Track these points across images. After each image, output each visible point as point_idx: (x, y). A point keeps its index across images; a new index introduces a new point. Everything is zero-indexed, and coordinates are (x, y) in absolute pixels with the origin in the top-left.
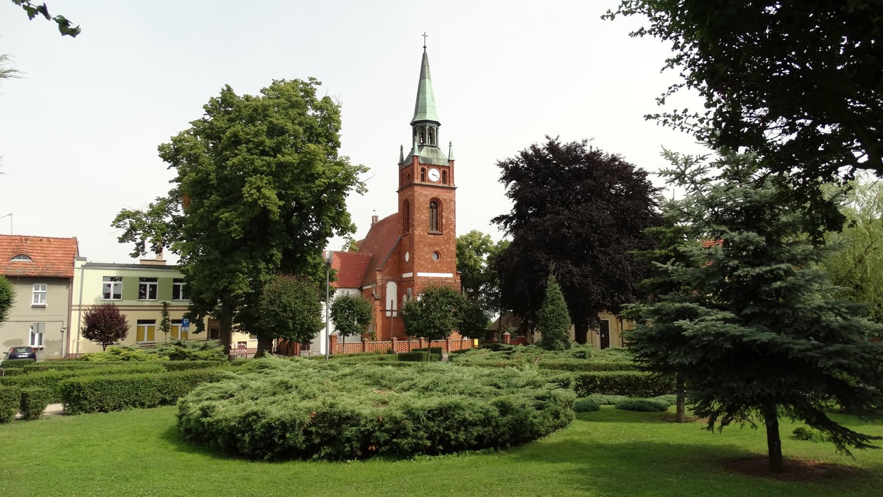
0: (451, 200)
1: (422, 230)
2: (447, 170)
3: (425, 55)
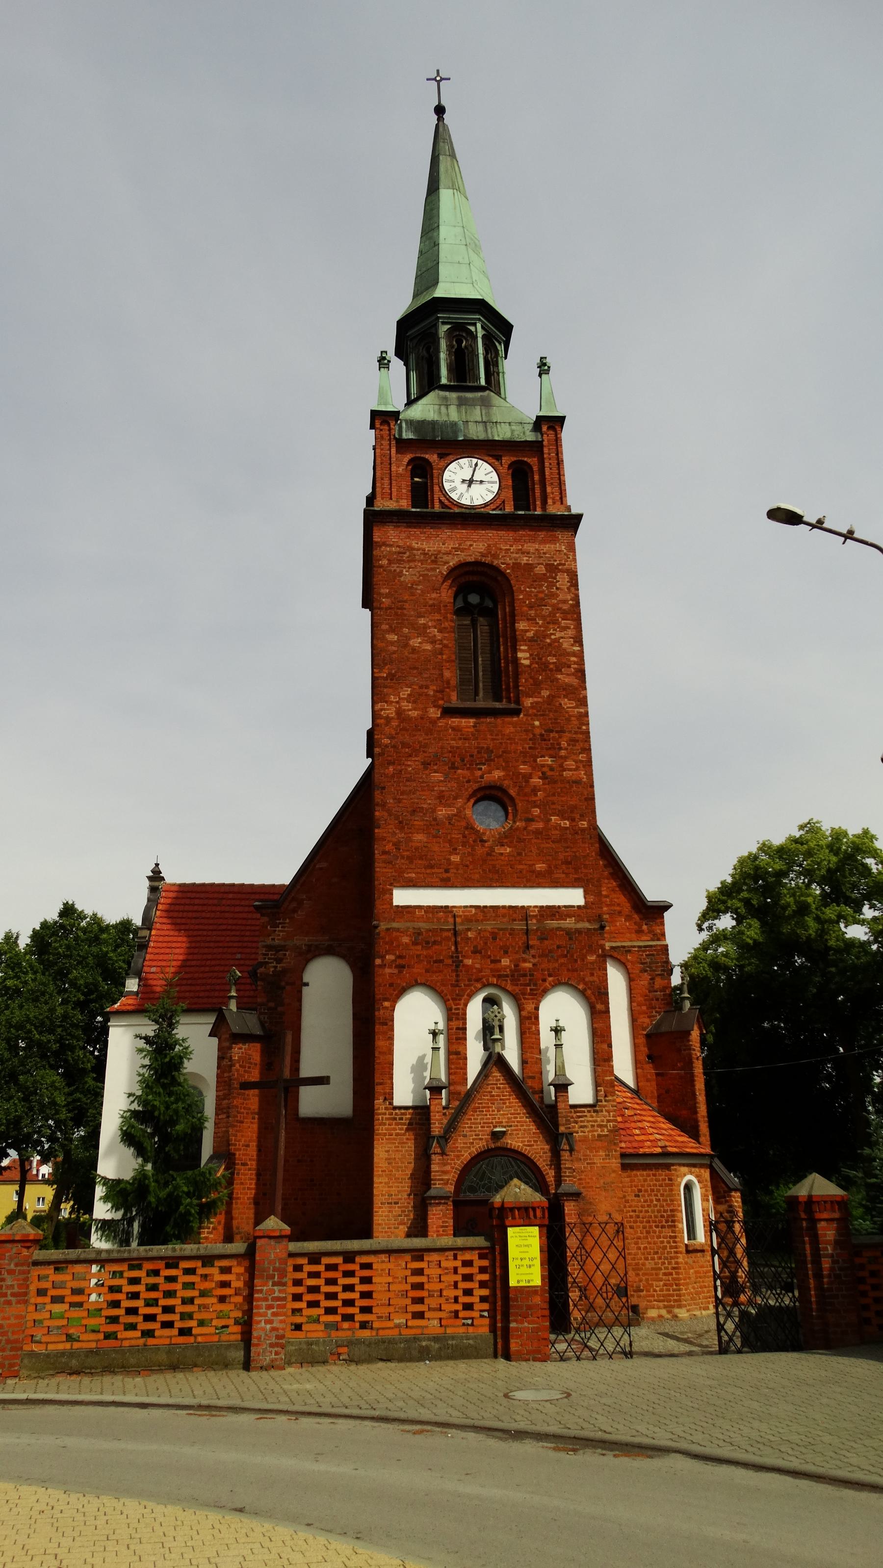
0: (553, 569)
1: (413, 698)
2: (533, 461)
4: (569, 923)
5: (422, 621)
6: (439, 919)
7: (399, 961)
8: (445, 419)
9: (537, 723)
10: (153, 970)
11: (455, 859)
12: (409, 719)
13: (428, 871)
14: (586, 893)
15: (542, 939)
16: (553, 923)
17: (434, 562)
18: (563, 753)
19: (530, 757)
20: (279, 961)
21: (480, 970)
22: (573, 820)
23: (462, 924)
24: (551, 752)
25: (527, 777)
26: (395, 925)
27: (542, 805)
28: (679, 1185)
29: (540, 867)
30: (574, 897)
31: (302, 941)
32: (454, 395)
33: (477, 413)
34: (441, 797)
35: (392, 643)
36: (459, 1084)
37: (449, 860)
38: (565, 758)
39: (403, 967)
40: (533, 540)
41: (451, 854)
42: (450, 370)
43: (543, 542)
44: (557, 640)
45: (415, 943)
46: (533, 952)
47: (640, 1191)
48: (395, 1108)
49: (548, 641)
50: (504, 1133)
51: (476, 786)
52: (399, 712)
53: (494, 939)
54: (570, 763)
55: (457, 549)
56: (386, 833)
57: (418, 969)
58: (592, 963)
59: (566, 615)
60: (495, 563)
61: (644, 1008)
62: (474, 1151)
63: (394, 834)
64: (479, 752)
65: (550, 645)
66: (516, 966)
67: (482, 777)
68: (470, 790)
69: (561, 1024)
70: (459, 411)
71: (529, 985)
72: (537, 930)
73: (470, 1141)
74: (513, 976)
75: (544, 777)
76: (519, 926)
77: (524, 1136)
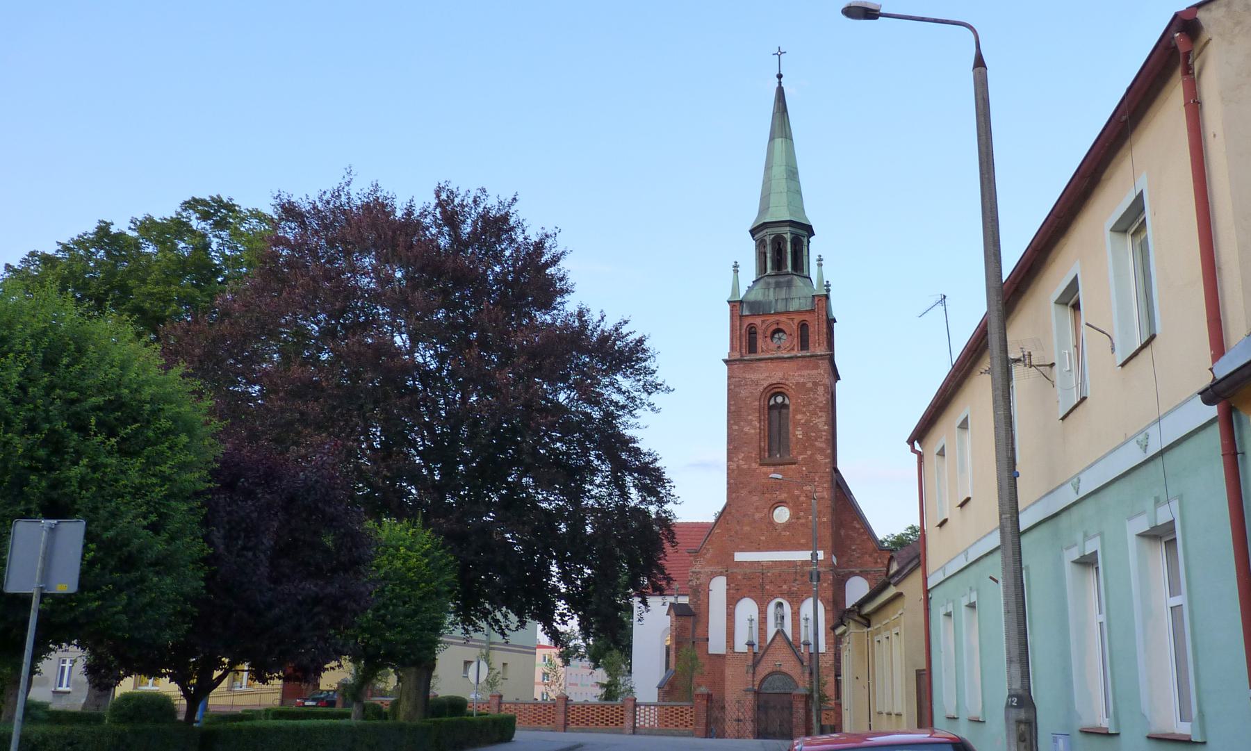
1: (746, 459)
3: (780, 92)
25: (798, 497)
29: (803, 541)
31: (709, 569)
32: (772, 280)
33: (783, 293)
34: (757, 508)
40: (807, 368)
42: (773, 261)
73: (764, 669)
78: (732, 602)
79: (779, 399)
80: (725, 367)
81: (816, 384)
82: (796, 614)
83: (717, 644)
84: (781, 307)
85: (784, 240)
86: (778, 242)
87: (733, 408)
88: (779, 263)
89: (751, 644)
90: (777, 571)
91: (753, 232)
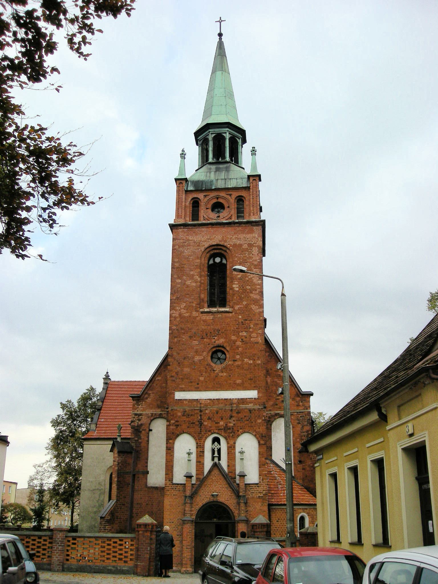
1: (186, 308)
4: (250, 406)
5: (192, 273)
6: (194, 405)
7: (176, 423)
8: (208, 179)
9: (240, 317)
10: (102, 420)
11: (202, 379)
12: (185, 317)
13: (190, 384)
14: (258, 393)
15: (238, 413)
16: (242, 406)
17: (199, 246)
18: (251, 330)
19: (236, 332)
20: (139, 420)
21: (211, 427)
22: (254, 360)
23: (203, 407)
24: (246, 330)
25: (234, 342)
26: (175, 408)
27: (241, 354)
28: (297, 517)
29: (239, 381)
30: (253, 394)
31: (149, 412)
32: (213, 167)
33: (223, 175)
34: (196, 352)
35: (179, 283)
36: (200, 475)
37: (199, 379)
38: (252, 332)
39: (178, 425)
40: (243, 232)
41: (200, 376)
43: (248, 233)
44: (251, 278)
45: (183, 415)
46: (233, 419)
47: (279, 519)
48: (173, 484)
49: (247, 279)
50: (217, 495)
51: (212, 346)
52: (180, 315)
53: (217, 413)
54: (254, 335)
55: (208, 239)
56: (174, 367)
57: (184, 426)
58: (260, 424)
59: (256, 266)
60: (225, 244)
61: (298, 440)
62: (204, 502)
63: (176, 368)
64: (214, 331)
65: (248, 281)
66: (226, 425)
67: (215, 342)
68: (210, 348)
69: (243, 450)
70: (215, 174)
71: (231, 433)
72: (236, 409)
73: (203, 498)
74: (225, 429)
75: (242, 341)
76: (228, 408)
77: (226, 497)
78: (171, 437)
79: (218, 260)
80: (169, 235)
81: (250, 245)
82: (231, 449)
83: (156, 477)
84: (221, 185)
85: (224, 139)
86: (219, 140)
87: (177, 265)
88: (219, 153)
89: (189, 477)
90: (215, 408)
91: (197, 134)
